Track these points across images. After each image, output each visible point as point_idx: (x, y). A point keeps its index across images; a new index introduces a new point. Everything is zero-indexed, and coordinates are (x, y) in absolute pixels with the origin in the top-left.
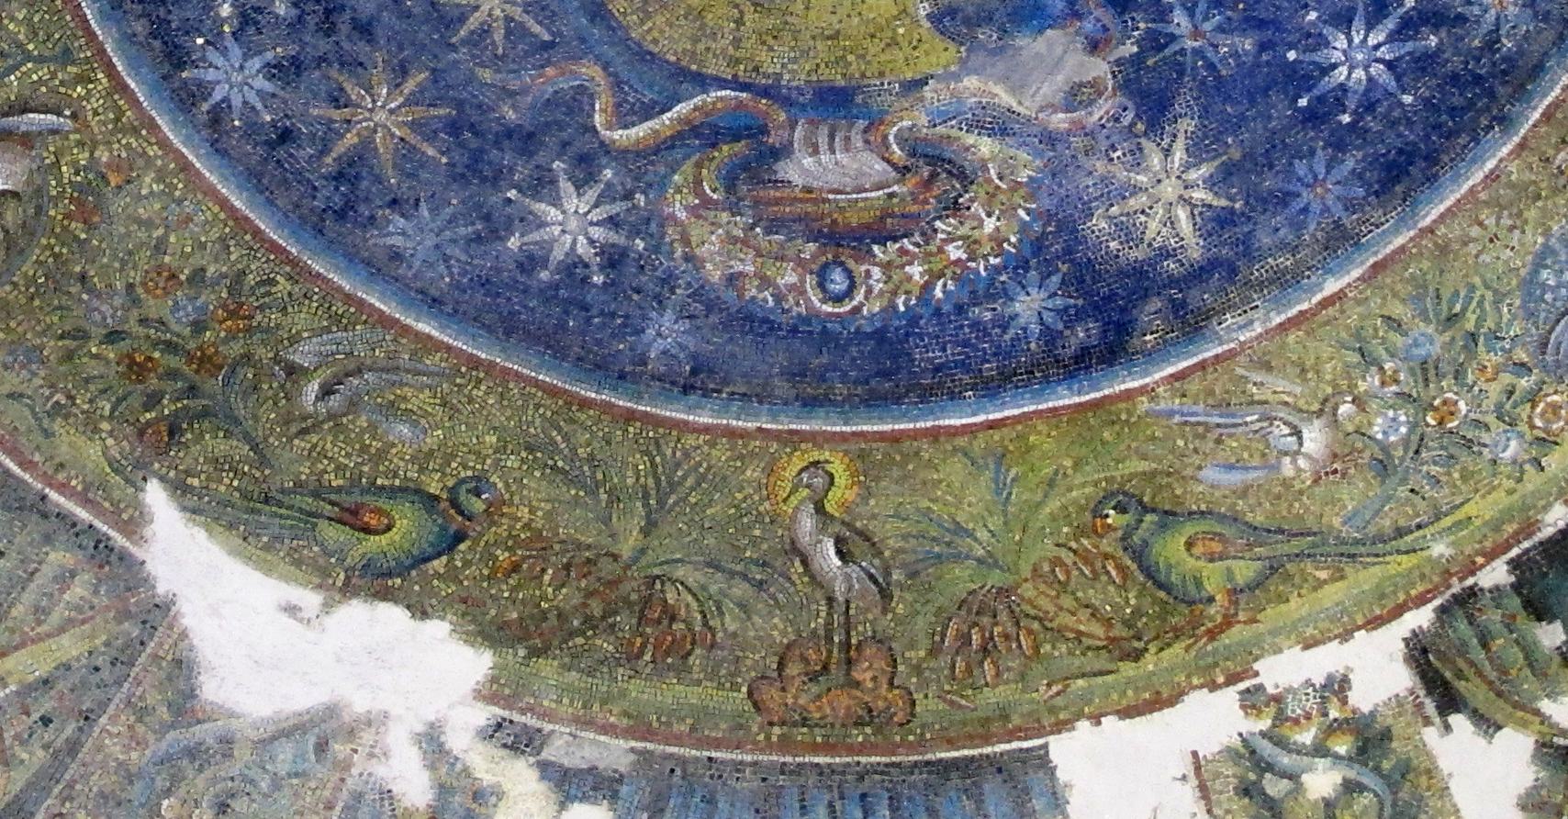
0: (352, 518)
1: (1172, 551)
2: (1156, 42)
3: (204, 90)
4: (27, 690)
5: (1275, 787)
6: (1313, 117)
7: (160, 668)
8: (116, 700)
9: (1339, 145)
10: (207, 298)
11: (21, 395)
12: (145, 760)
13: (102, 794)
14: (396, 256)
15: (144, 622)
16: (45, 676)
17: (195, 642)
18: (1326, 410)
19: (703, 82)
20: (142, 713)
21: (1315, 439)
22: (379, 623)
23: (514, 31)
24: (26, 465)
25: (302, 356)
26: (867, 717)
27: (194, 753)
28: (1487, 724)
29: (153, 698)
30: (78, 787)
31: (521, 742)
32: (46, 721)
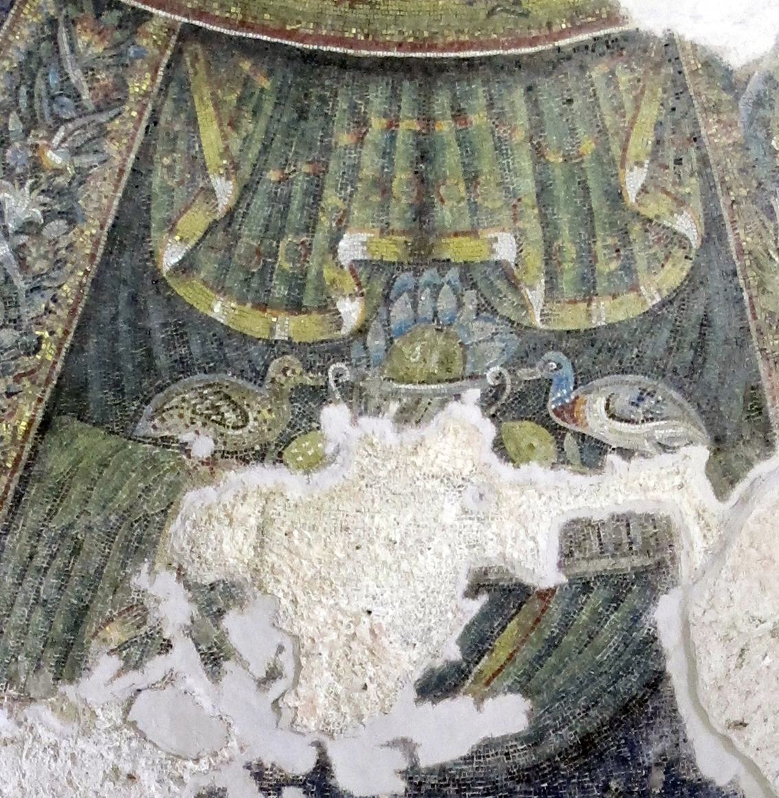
4: (654, 155)
7: (702, 76)
8: (698, 115)
11: (493, 9)
12: (742, 131)
13: (741, 170)
15: (670, 61)
16: (653, 139)
17: (703, 43)
20: (716, 108)
24: (533, 42)
29: (714, 95)
30: (727, 179)
32: (678, 162)
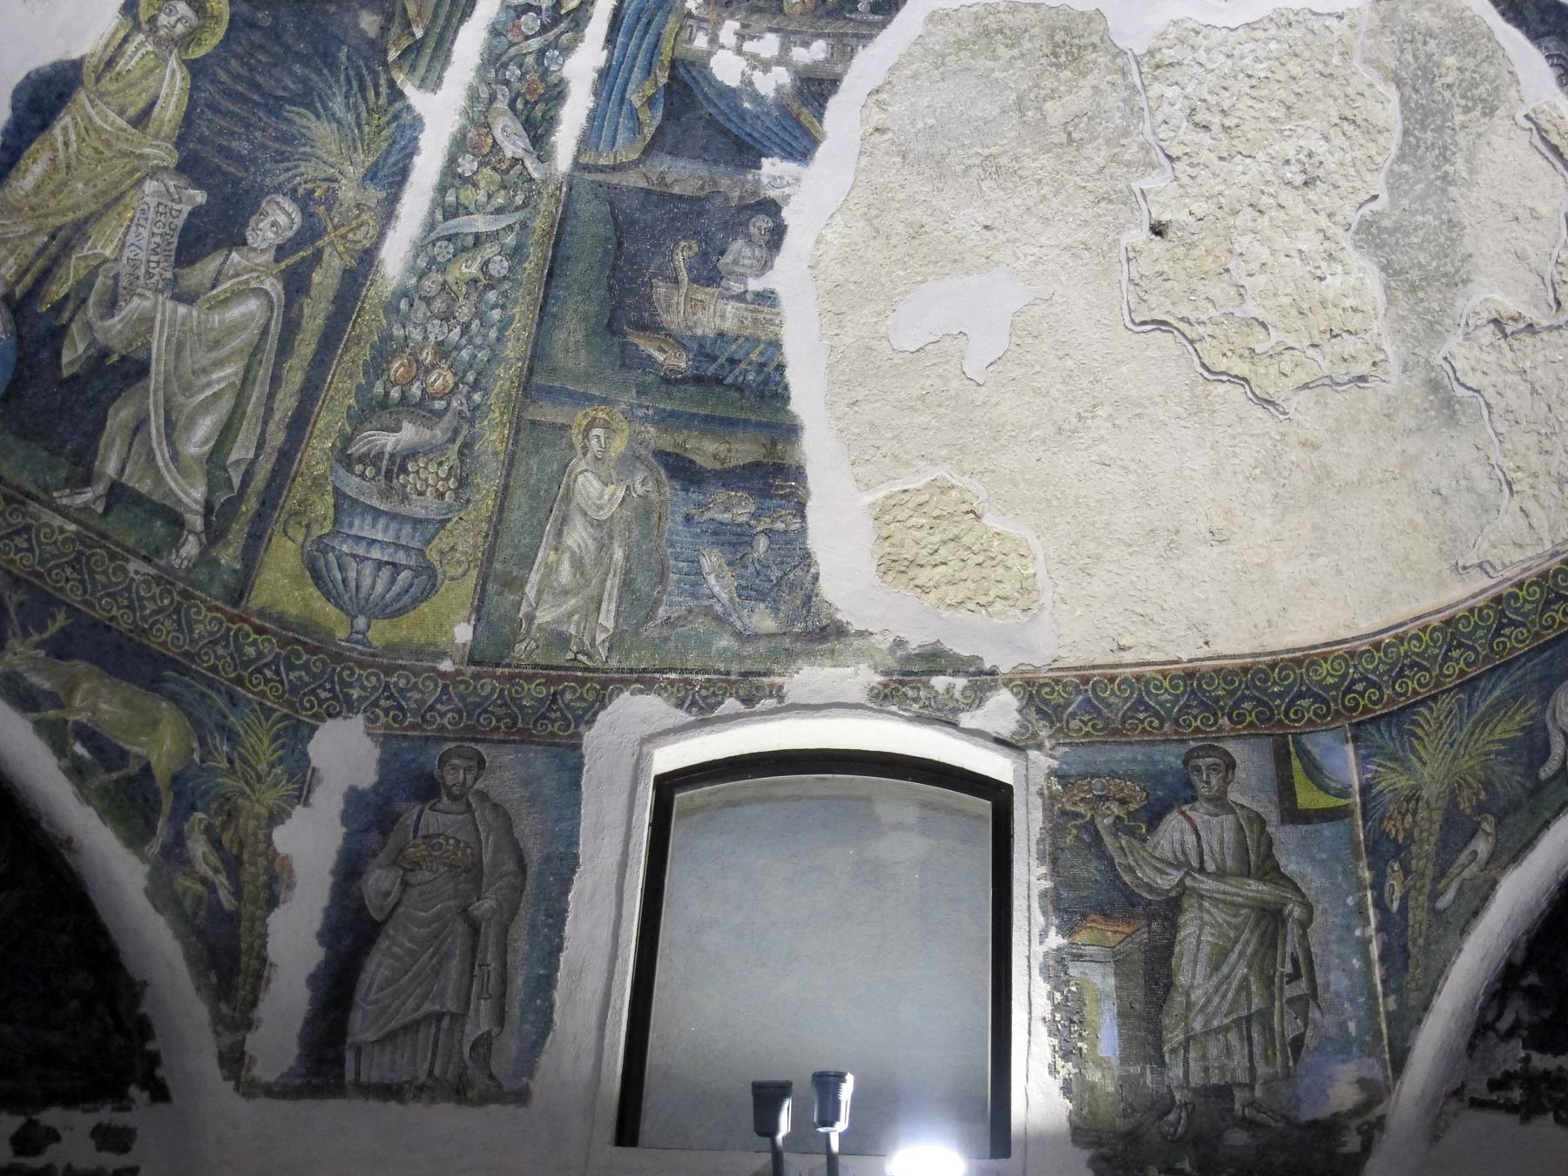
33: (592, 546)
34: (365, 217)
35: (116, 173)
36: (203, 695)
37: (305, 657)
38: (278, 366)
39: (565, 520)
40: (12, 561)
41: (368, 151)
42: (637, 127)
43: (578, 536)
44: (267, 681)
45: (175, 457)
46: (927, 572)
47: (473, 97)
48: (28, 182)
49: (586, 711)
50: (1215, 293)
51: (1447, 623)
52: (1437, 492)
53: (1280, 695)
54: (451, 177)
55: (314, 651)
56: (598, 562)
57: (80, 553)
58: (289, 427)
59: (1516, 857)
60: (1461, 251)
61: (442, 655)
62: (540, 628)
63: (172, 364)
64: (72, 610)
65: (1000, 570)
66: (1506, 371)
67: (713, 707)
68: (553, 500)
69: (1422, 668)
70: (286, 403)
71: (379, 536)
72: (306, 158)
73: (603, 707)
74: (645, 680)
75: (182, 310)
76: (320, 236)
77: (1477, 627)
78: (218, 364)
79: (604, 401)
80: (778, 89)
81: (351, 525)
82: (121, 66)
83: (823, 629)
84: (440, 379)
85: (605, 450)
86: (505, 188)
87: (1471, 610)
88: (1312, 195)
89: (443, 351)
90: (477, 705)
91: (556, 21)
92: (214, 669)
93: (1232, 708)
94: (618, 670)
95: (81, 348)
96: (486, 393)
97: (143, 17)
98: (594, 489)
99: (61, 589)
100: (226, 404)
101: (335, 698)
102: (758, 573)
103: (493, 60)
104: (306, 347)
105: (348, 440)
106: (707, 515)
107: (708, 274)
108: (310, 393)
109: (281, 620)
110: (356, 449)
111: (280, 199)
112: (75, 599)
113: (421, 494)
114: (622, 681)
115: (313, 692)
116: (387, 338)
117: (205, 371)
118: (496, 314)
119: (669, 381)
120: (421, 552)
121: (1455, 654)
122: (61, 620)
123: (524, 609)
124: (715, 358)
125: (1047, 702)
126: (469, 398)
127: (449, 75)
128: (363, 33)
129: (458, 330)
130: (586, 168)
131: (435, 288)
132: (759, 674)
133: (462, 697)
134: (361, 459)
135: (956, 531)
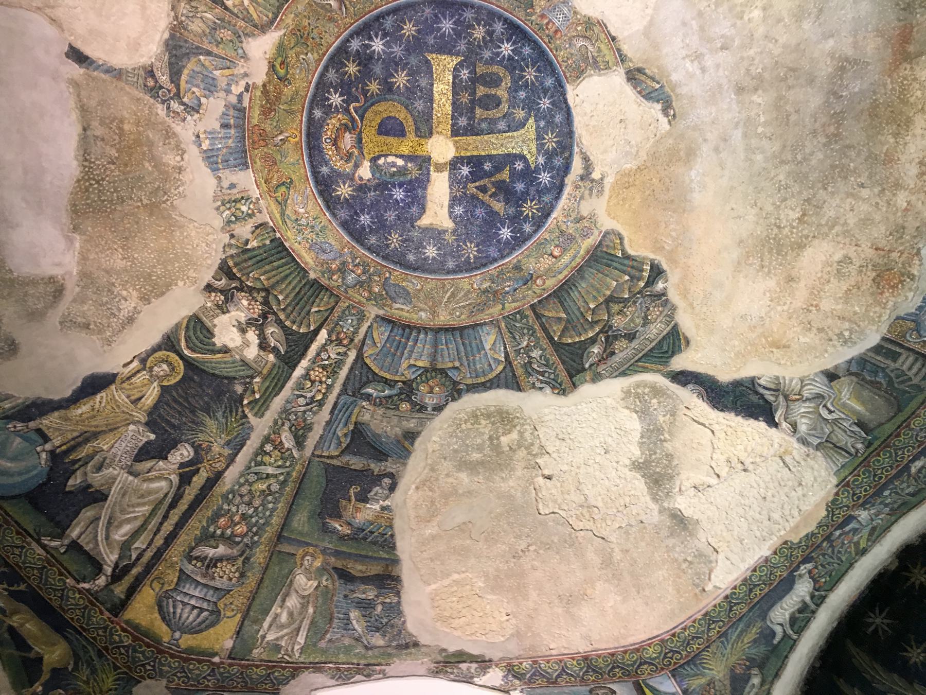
0: (282, 63)
1: (283, 189)
2: (370, 190)
3: (353, 39)
4: (247, 10)
5: (243, 202)
6: (356, 213)
9: (351, 216)
10: (318, 40)
14: (328, 71)
18: (306, 212)
19: (362, 121)
21: (302, 211)
22: (264, 68)
23: (368, 91)
25: (309, 54)
26: (254, 142)
27: (240, 36)
28: (253, 232)
31: (247, 90)
33: (299, 606)
34: (221, 459)
35: (118, 419)
36: (84, 646)
37: (144, 648)
38: (168, 512)
39: (287, 595)
40: (8, 557)
41: (228, 435)
42: (340, 443)
43: (293, 602)
44: (121, 654)
45: (107, 537)
46: (457, 621)
47: (276, 422)
48: (79, 411)
49: (284, 680)
50: (576, 499)
51: (706, 614)
52: (686, 560)
53: (632, 665)
54: (261, 451)
55: (148, 646)
56: (300, 614)
57: (45, 567)
58: (166, 539)
59: (777, 675)
60: (674, 463)
61: (216, 654)
62: (268, 643)
63: (119, 500)
64: (29, 586)
65: (491, 618)
66: (704, 504)
67: (349, 679)
68: (283, 585)
69: (698, 638)
70: (168, 527)
71: (197, 594)
72: (202, 432)
73: (293, 678)
74: (317, 667)
75: (131, 478)
76: (201, 463)
77: (720, 612)
78: (139, 505)
79: (312, 545)
80: (396, 435)
81: (184, 587)
82: (133, 380)
83: (407, 644)
84: (241, 529)
85: (311, 566)
86: (282, 458)
87: (715, 606)
88: (607, 456)
89: (244, 517)
90: (227, 677)
91: (311, 403)
92: (94, 638)
93: (609, 672)
94: (303, 663)
95: (78, 481)
96: (260, 537)
97: (148, 365)
98: (303, 582)
99: (29, 578)
100: (138, 523)
101: (154, 670)
102: (377, 620)
103: (285, 412)
104: (183, 506)
105: (192, 549)
106: (355, 595)
107: (363, 498)
108: (179, 525)
109: (137, 627)
110: (195, 553)
111: (187, 445)
112: (34, 584)
113: (222, 577)
114: (304, 668)
115: (143, 665)
116: (220, 508)
117: (133, 506)
118: (270, 506)
119: (342, 538)
120: (215, 603)
121: (713, 626)
122: (22, 587)
123: (261, 633)
124: (364, 530)
125: (517, 673)
126: (252, 538)
127: (268, 414)
128: (235, 392)
129: (252, 509)
130: (318, 456)
131: (246, 492)
132: (374, 665)
133: (221, 674)
134: (197, 558)
135: (470, 603)
